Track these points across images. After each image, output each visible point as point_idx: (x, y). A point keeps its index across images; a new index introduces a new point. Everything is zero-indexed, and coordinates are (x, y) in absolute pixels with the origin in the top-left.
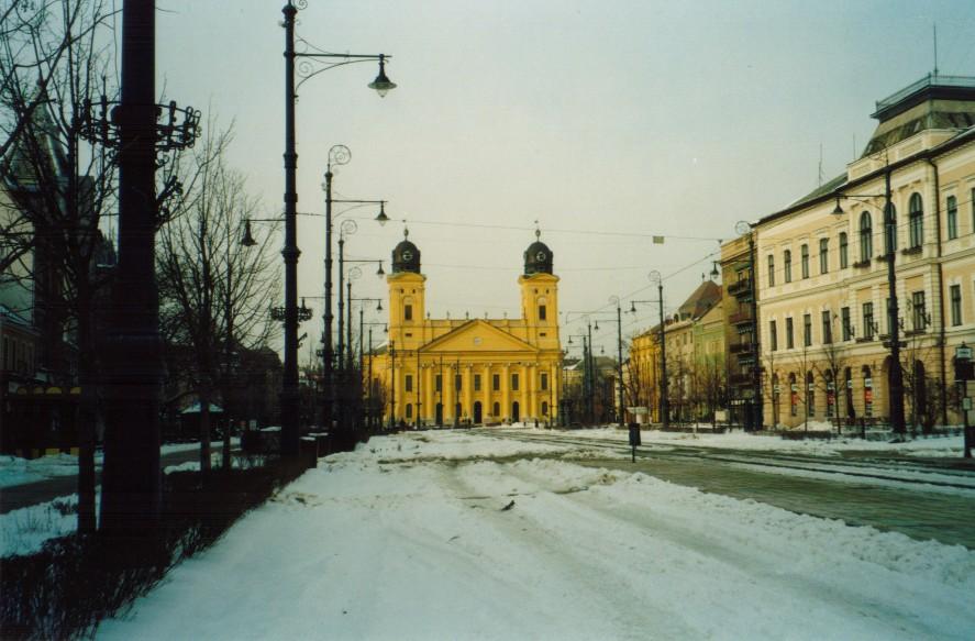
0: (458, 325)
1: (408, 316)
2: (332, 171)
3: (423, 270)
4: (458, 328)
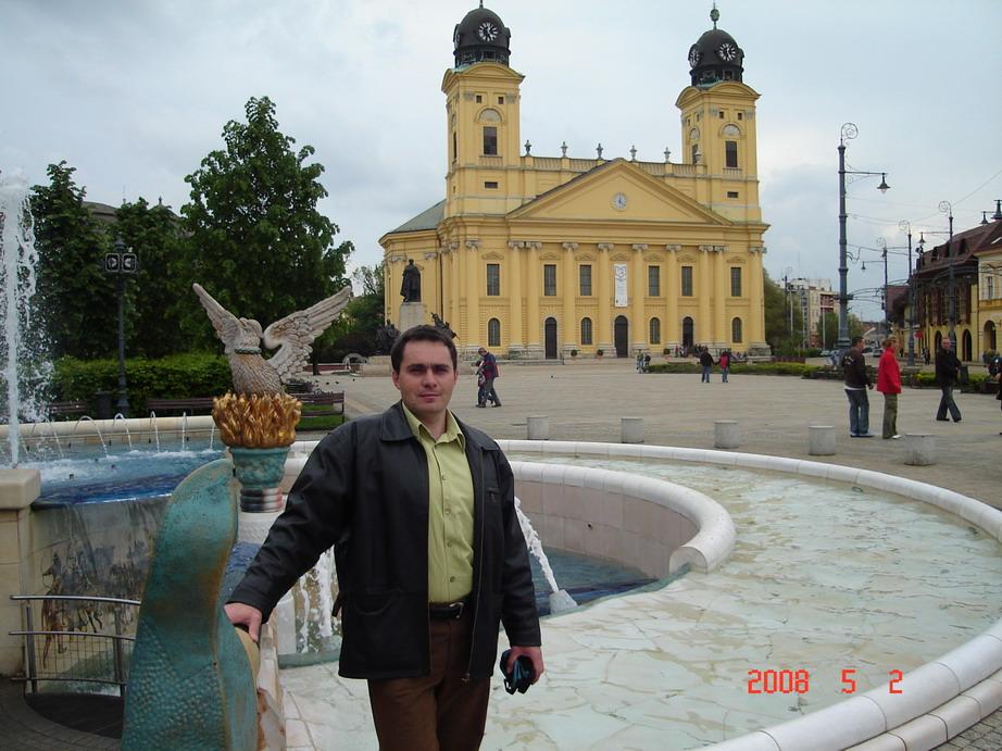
0: (586, 169)
1: (490, 146)
2: (844, 144)
3: (516, 63)
4: (584, 174)
